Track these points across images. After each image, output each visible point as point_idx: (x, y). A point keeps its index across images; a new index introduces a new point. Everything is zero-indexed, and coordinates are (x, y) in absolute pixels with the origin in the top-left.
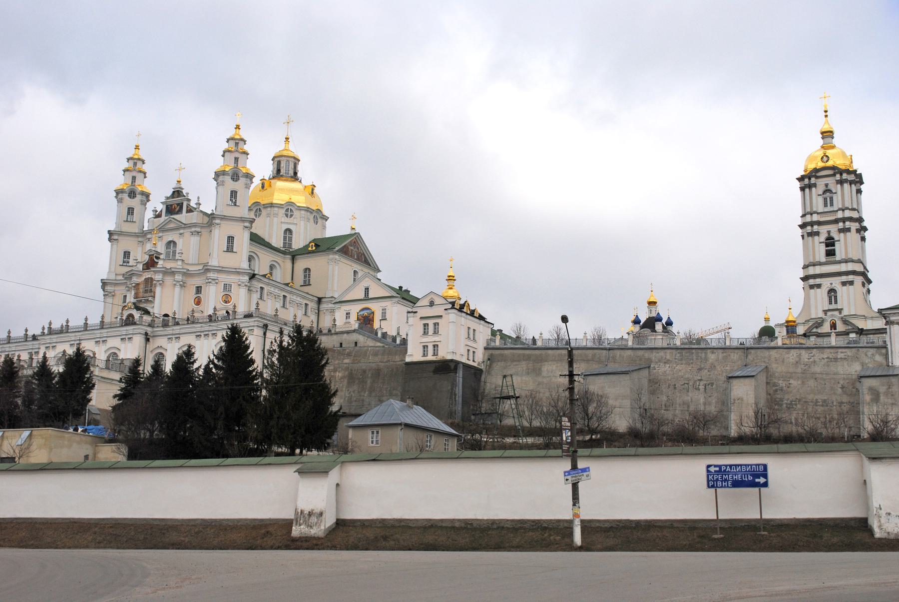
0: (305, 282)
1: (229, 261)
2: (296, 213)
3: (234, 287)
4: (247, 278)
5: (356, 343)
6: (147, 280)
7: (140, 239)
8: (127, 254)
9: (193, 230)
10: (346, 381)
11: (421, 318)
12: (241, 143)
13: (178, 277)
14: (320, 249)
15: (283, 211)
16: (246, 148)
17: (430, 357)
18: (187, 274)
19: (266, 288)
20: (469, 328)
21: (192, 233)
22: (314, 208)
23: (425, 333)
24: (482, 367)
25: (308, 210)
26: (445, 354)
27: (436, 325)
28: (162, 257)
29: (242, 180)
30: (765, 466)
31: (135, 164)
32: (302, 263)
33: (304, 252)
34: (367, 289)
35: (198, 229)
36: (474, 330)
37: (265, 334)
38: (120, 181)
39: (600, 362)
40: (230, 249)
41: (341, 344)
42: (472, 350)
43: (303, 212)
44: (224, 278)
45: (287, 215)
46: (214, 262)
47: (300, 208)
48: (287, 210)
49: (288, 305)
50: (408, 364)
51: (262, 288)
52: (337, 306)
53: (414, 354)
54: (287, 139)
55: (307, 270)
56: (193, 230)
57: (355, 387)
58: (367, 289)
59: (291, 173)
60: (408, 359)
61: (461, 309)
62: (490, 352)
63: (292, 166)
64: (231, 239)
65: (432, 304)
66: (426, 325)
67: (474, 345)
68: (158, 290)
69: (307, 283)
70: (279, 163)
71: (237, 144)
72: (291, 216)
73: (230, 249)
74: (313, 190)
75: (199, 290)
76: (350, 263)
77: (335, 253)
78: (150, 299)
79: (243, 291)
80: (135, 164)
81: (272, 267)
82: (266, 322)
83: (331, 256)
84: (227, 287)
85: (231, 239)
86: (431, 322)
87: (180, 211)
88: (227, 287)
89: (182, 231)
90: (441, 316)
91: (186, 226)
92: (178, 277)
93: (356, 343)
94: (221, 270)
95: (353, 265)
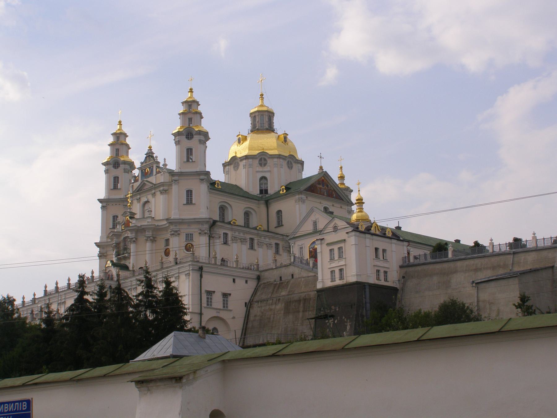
0: (278, 222)
1: (190, 214)
2: (269, 161)
3: (196, 237)
4: (206, 227)
5: (292, 275)
8: (115, 217)
9: (162, 188)
10: (282, 312)
11: (328, 244)
14: (292, 190)
15: (257, 161)
16: (200, 109)
17: (338, 282)
18: (157, 230)
19: (230, 234)
20: (376, 249)
22: (287, 154)
23: (332, 259)
24: (397, 285)
25: (279, 156)
26: (351, 277)
27: (340, 249)
28: (137, 216)
29: (196, 138)
30: (29, 402)
32: (275, 207)
33: (277, 196)
34: (315, 223)
35: (166, 188)
36: (384, 251)
37: (201, 276)
38: (106, 154)
39: (494, 268)
40: (189, 201)
41: (281, 277)
42: (382, 270)
43: (275, 160)
44: (185, 230)
45: (261, 165)
46: (174, 215)
47: (272, 157)
48: (261, 160)
49: (256, 246)
50: (320, 291)
51: (226, 235)
52: (291, 242)
53: (325, 280)
54: (262, 95)
55: (279, 212)
56: (162, 188)
57: (291, 316)
58: (315, 223)
59: (266, 126)
60: (319, 286)
61: (368, 231)
62: (405, 270)
63: (266, 119)
64: (189, 193)
65: (336, 229)
66: (331, 250)
67: (386, 265)
68: (132, 247)
69: (280, 224)
72: (265, 165)
73: (189, 201)
74: (285, 138)
75: (167, 241)
76: (319, 201)
77: (300, 193)
78: (126, 255)
79: (204, 240)
81: (247, 214)
82: (201, 265)
83: (297, 197)
84: (189, 237)
85: (189, 193)
86: (336, 247)
87: (151, 173)
88: (189, 237)
89: (153, 191)
90: (345, 240)
91: (155, 186)
92: (149, 234)
93: (292, 275)
94: (181, 222)
95: (322, 201)
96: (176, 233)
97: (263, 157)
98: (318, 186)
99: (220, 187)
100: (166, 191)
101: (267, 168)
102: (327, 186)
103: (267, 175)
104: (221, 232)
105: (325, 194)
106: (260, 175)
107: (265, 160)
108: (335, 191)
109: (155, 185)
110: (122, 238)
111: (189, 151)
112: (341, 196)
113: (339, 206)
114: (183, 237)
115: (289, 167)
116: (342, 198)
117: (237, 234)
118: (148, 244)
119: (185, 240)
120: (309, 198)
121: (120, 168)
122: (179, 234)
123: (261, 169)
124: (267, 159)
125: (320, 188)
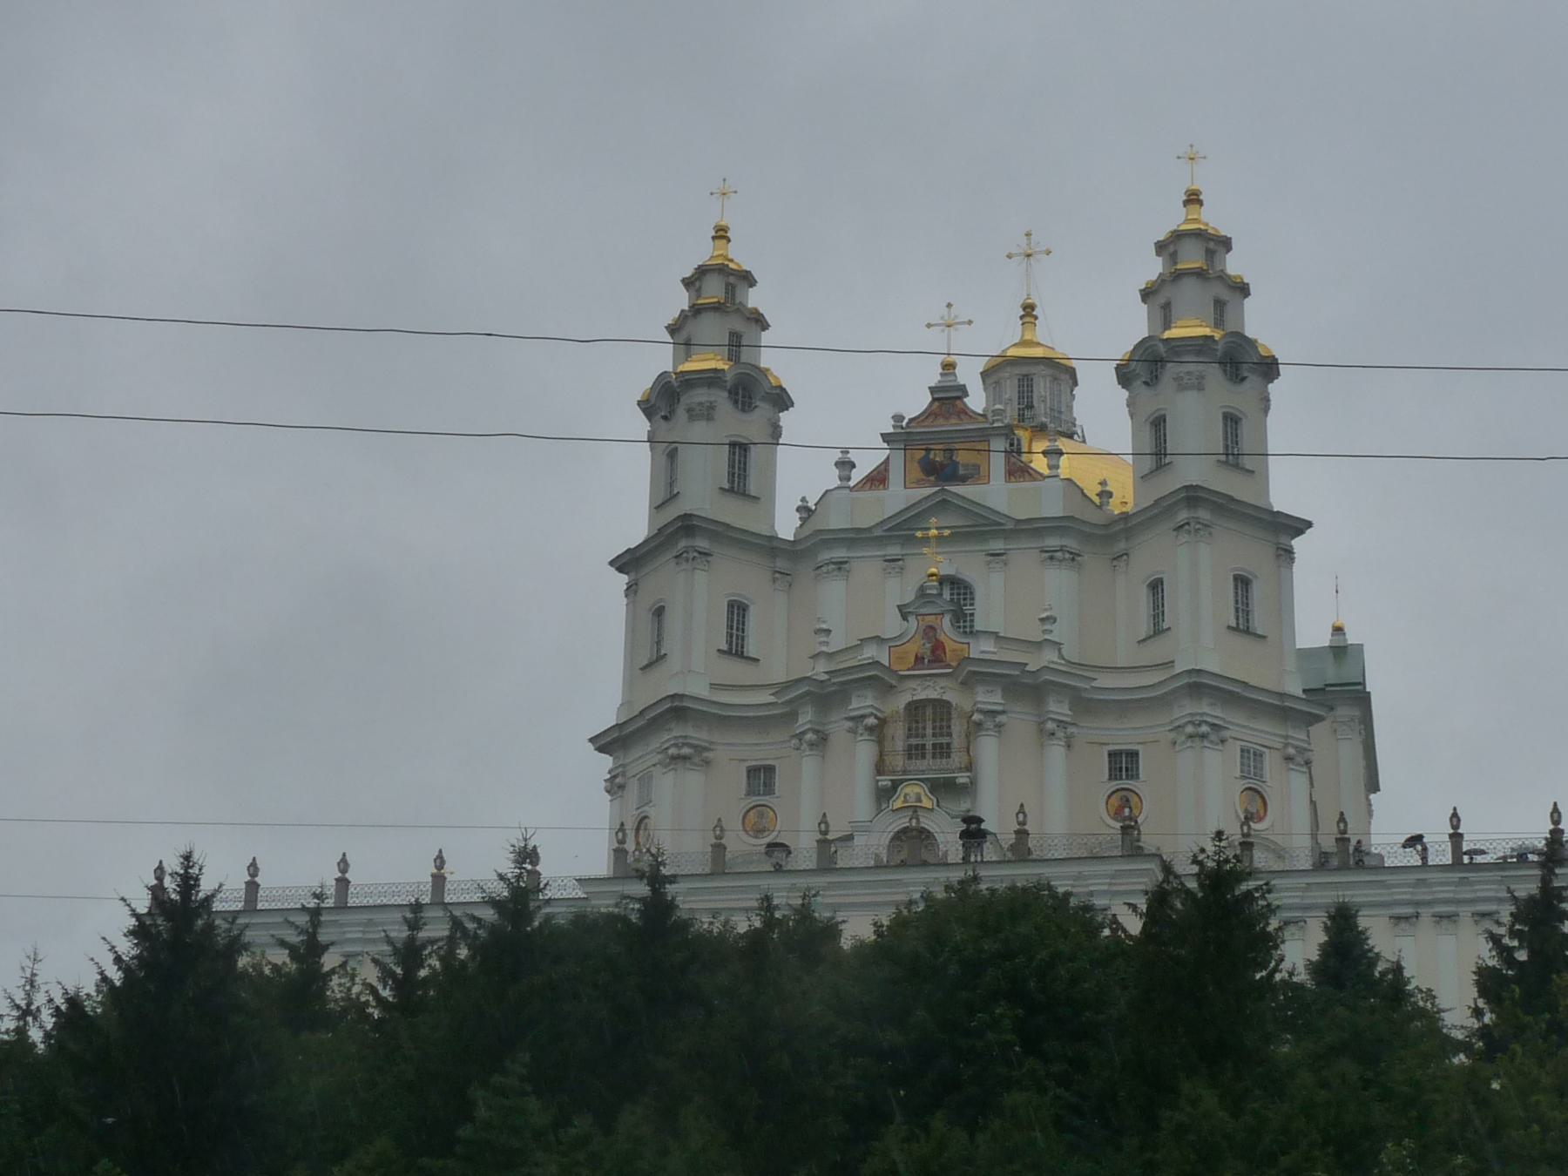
3: (1271, 763)
6: (915, 708)
7: (781, 564)
12: (1222, 249)
13: (1058, 708)
18: (1085, 704)
21: (1051, 556)
31: (730, 290)
56: (1053, 542)
68: (988, 749)
70: (1026, 383)
71: (1210, 254)
78: (962, 778)
80: (730, 290)
88: (1252, 758)
89: (997, 545)
96: (1208, 735)
100: (1074, 556)
109: (1019, 521)
110: (901, 701)
114: (1234, 749)
118: (1056, 752)
119: (1238, 774)
121: (757, 412)
122: (1223, 741)
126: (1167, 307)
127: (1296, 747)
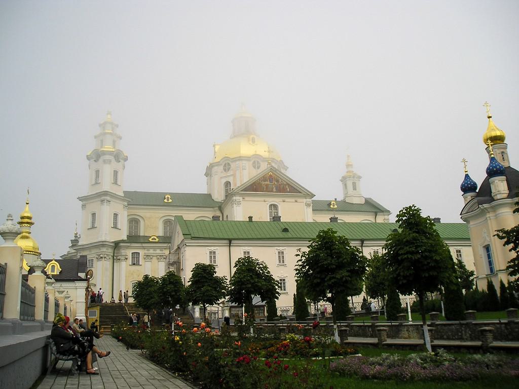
2: (233, 165)
15: (222, 168)
19: (142, 253)
51: (136, 256)
72: (229, 169)
76: (262, 199)
79: (107, 264)
95: (266, 199)
97: (227, 162)
98: (263, 183)
99: (170, 201)
101: (231, 173)
102: (277, 181)
103: (231, 179)
104: (129, 253)
105: (274, 190)
106: (224, 181)
107: (229, 164)
108: (288, 184)
111: (97, 172)
112: (298, 189)
113: (293, 200)
115: (254, 167)
116: (300, 190)
117: (151, 251)
120: (247, 198)
123: (224, 174)
124: (230, 163)
125: (267, 185)
126: (102, 141)
127: (107, 254)
